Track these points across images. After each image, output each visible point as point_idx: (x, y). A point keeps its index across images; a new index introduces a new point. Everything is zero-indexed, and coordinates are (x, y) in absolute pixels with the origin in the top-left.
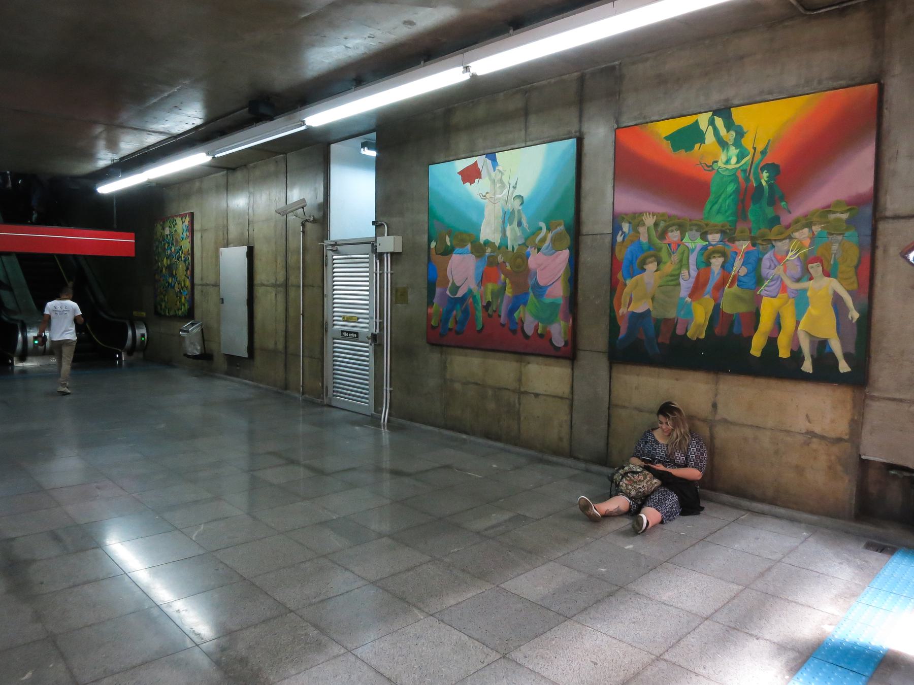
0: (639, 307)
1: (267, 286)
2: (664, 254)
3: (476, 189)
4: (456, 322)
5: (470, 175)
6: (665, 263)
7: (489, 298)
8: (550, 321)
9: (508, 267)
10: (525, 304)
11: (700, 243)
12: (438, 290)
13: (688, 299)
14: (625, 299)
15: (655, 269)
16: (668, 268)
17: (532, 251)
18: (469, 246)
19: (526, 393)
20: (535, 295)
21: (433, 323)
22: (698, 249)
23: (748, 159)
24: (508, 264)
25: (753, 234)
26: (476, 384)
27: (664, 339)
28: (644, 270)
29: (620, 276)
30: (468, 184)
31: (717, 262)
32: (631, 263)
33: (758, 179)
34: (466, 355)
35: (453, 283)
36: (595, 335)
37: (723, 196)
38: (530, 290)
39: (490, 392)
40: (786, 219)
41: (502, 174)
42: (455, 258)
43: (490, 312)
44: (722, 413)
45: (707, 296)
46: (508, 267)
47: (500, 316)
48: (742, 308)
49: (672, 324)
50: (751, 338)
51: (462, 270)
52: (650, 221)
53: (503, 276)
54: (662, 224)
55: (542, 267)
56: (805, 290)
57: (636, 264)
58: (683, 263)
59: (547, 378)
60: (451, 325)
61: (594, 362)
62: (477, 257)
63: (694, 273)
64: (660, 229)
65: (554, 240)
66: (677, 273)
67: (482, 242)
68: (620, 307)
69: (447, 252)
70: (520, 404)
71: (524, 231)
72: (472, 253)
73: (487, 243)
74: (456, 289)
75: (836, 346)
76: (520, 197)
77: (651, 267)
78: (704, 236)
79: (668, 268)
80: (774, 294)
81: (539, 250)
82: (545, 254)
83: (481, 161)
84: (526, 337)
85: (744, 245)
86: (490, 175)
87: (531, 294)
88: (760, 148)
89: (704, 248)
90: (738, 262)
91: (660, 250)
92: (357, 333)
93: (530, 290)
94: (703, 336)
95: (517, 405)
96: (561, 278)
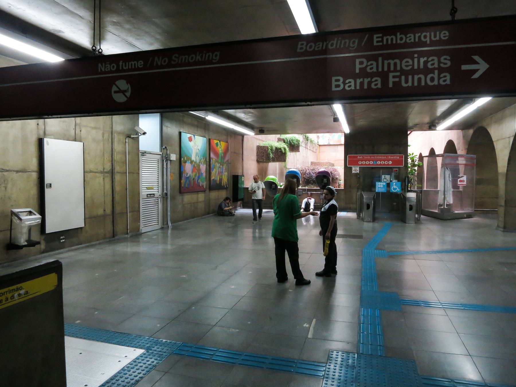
1: (96, 172)
3: (191, 144)
8: (203, 182)
60: (186, 186)
69: (185, 162)
74: (187, 174)
92: (154, 194)
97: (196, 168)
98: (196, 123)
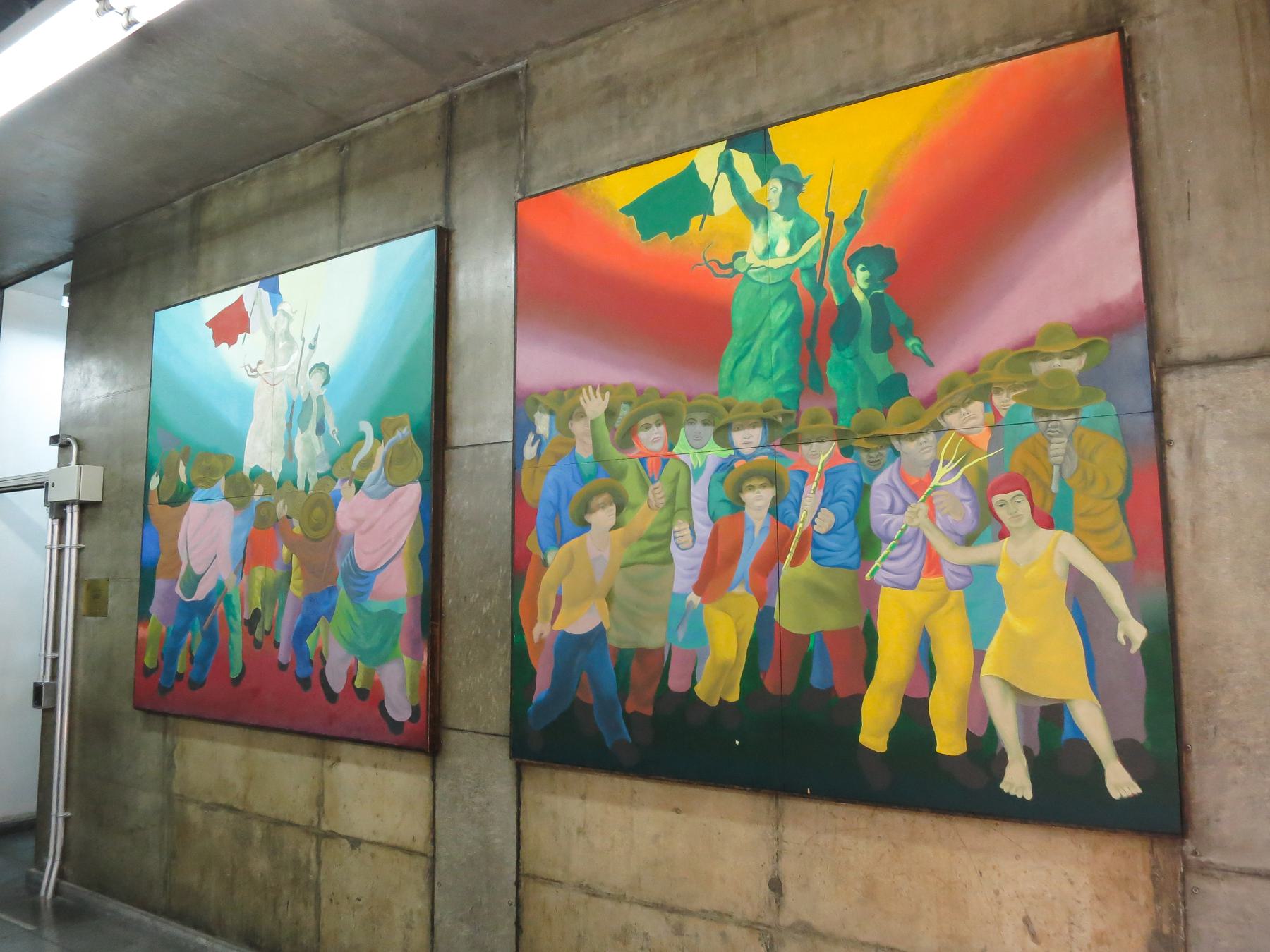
0: (579, 622)
2: (630, 485)
4: (192, 659)
5: (229, 326)
6: (635, 507)
7: (257, 602)
8: (378, 656)
9: (297, 530)
10: (329, 615)
11: (714, 453)
12: (160, 585)
13: (695, 599)
14: (545, 600)
15: (613, 522)
16: (643, 518)
17: (345, 489)
18: (222, 483)
19: (332, 835)
20: (349, 593)
21: (149, 661)
22: (711, 466)
23: (815, 240)
24: (295, 522)
25: (842, 424)
26: (231, 809)
27: (641, 703)
28: (586, 526)
29: (532, 543)
30: (225, 345)
31: (758, 500)
32: (557, 510)
33: (844, 287)
34: (213, 739)
35: (189, 568)
36: (481, 695)
37: (762, 336)
38: (340, 582)
39: (258, 831)
40: (923, 381)
41: (290, 319)
42: (195, 510)
43: (258, 634)
44: (796, 905)
45: (740, 590)
46: (297, 530)
47: (277, 645)
48: (831, 620)
49: (658, 662)
50: (858, 699)
51: (207, 537)
52: (595, 406)
53: (285, 550)
54: (624, 412)
55: (364, 527)
56: (991, 566)
57: (567, 515)
58: (677, 506)
59: (376, 796)
60: (181, 666)
61: (480, 759)
62: (237, 507)
63: (704, 531)
64: (619, 424)
65: (389, 462)
66: (663, 530)
67: (246, 472)
68: (534, 622)
69: (180, 498)
70: (319, 863)
71: (328, 443)
72: (226, 498)
73: (257, 474)
74: (193, 581)
75: (1091, 722)
76: (323, 367)
77: (602, 517)
78: (722, 434)
79: (643, 518)
80: (908, 579)
81: (359, 486)
82: (370, 495)
83: (251, 294)
84: (331, 696)
85: (821, 455)
86: (266, 324)
87: (342, 591)
88: (843, 210)
89: (725, 466)
90: (811, 497)
91: (621, 475)
93: (340, 582)
94: (734, 697)
95: (314, 866)
96: (406, 549)
97: (291, 524)
98: (321, 171)
